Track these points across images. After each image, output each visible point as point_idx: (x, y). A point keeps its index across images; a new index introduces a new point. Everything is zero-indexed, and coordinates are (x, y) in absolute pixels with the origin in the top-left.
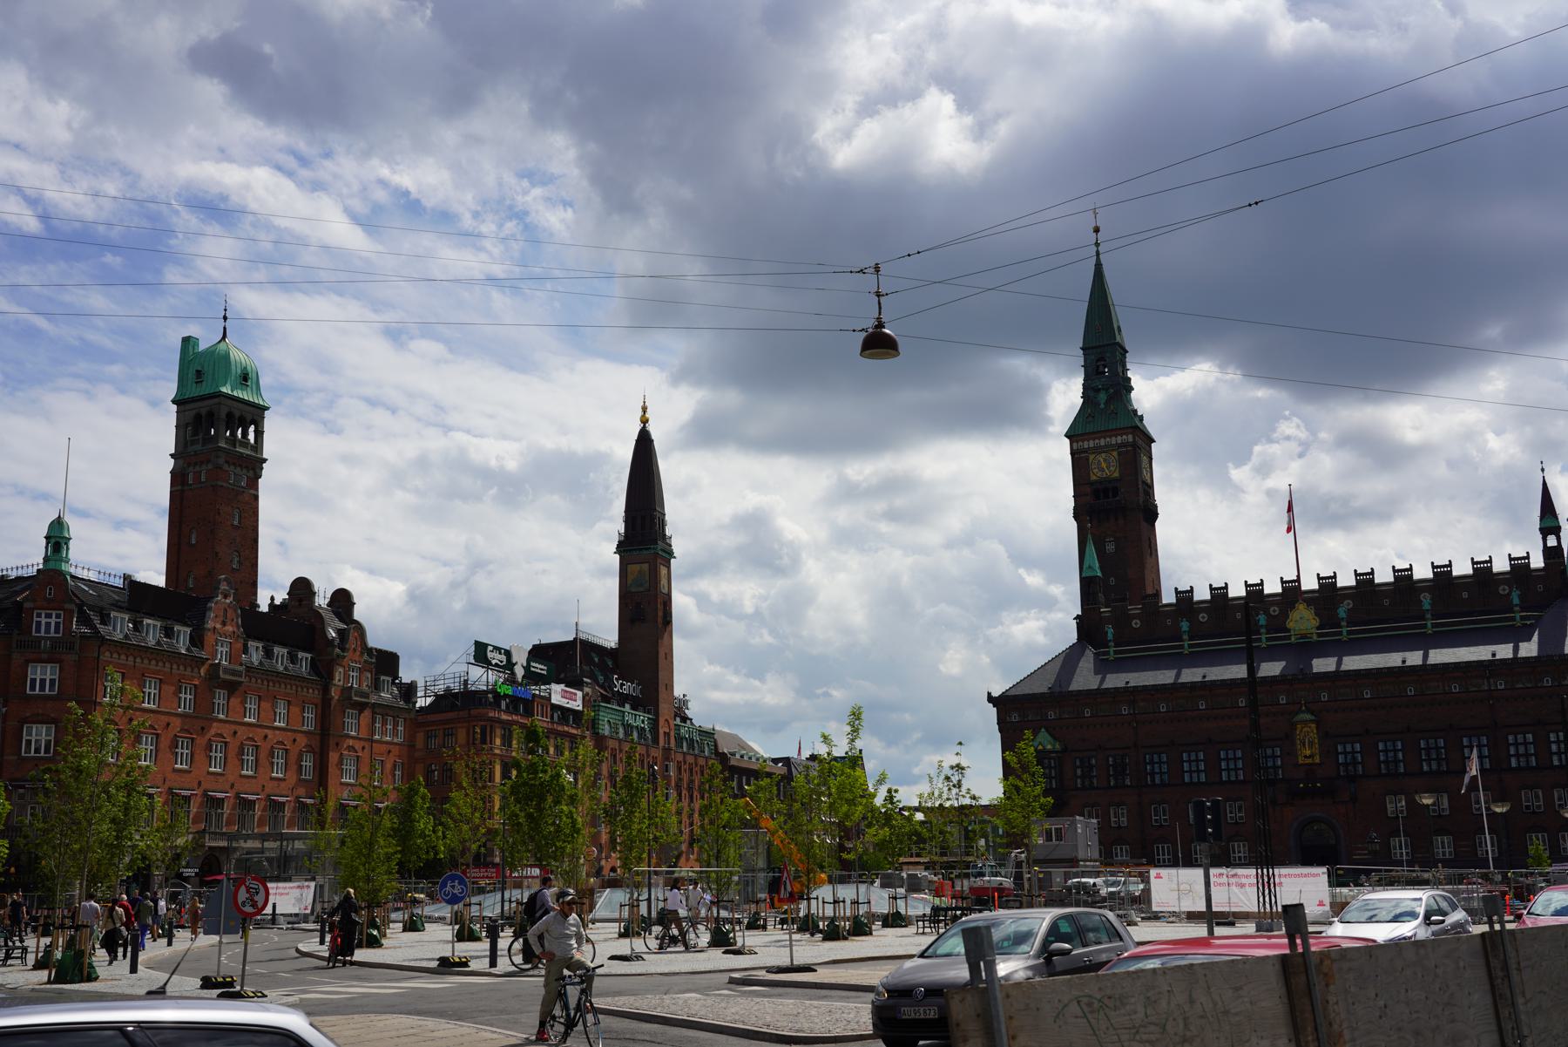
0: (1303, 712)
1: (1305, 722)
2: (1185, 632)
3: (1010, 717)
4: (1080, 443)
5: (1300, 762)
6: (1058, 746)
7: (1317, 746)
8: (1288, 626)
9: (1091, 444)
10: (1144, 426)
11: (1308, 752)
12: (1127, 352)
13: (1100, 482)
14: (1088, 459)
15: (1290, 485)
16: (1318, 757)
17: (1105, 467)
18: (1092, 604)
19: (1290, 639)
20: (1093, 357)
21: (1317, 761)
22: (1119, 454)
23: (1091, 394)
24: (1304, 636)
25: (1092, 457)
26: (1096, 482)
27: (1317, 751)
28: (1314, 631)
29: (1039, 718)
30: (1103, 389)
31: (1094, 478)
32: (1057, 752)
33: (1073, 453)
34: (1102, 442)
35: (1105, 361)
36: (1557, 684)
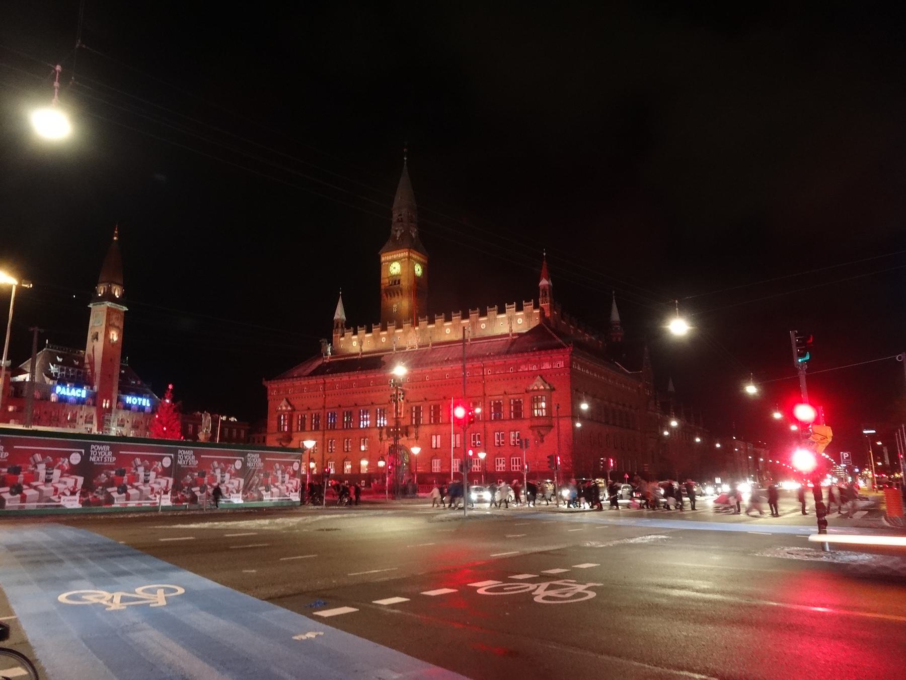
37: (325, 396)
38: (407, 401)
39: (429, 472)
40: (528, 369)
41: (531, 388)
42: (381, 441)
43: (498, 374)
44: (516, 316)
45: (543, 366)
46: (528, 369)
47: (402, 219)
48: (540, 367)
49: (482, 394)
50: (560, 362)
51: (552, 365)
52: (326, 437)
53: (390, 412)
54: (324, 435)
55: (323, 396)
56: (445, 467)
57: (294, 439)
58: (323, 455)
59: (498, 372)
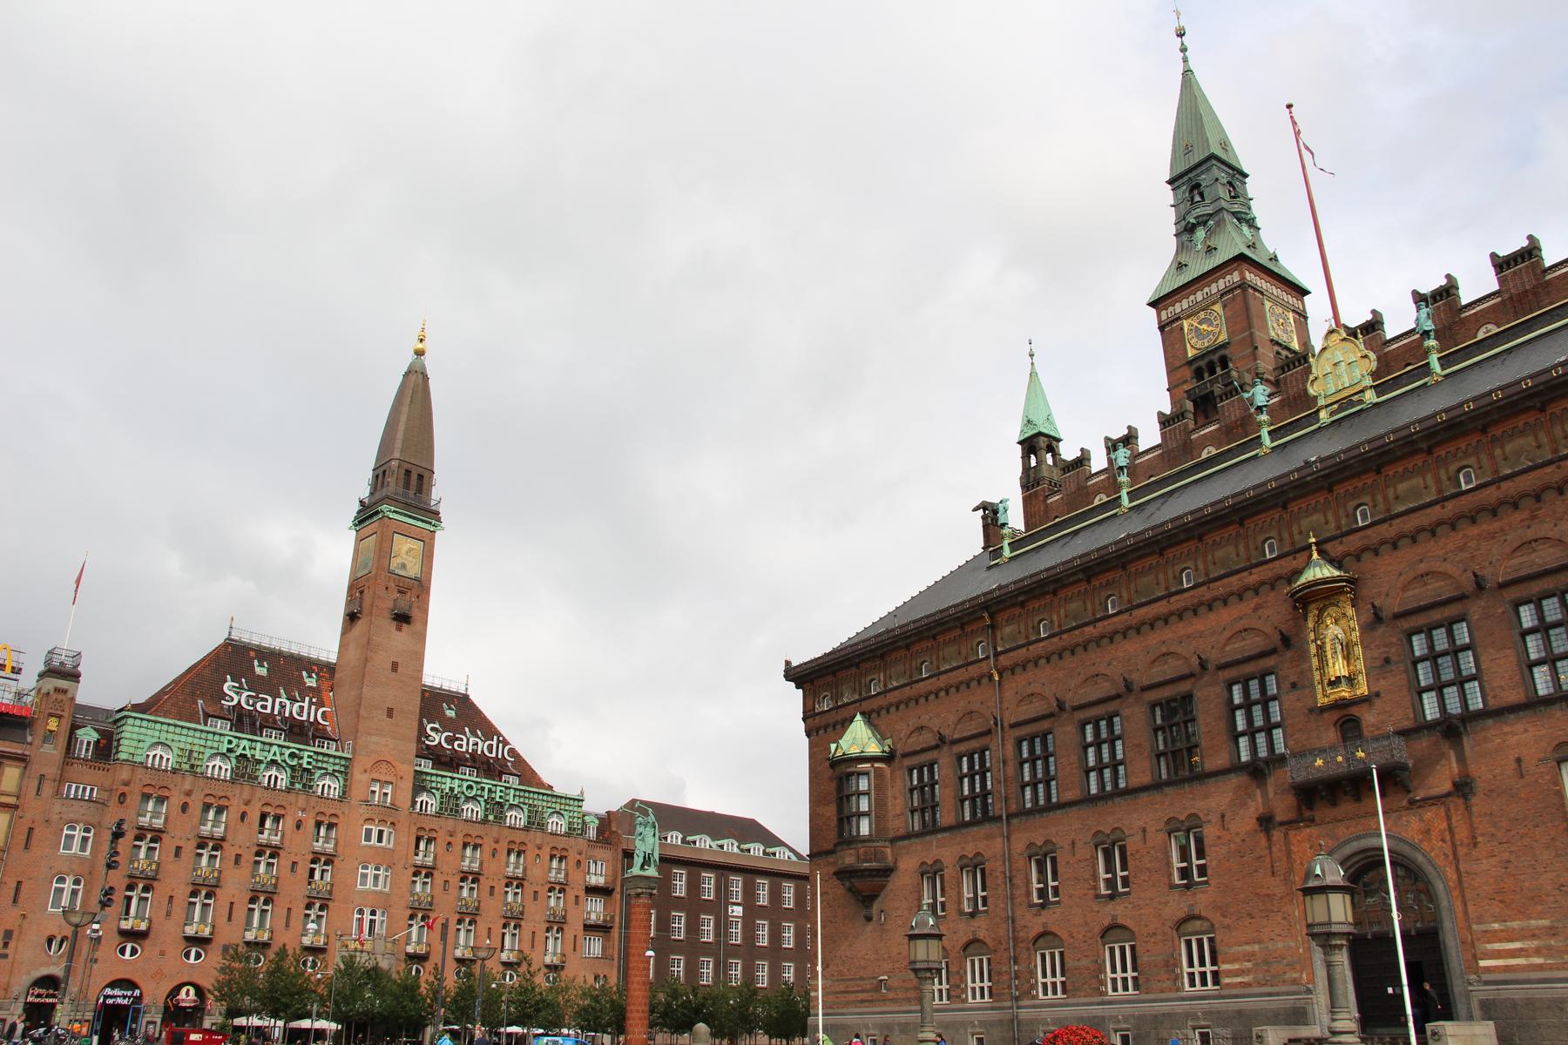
1: (1321, 595)
2: (1121, 468)
3: (819, 703)
4: (1171, 309)
5: (1322, 701)
6: (874, 748)
7: (1358, 650)
8: (1312, 391)
9: (1185, 303)
10: (1281, 267)
11: (1338, 668)
12: (1246, 176)
14: (1182, 329)
15: (1289, 106)
16: (1362, 679)
18: (1033, 486)
19: (1318, 420)
21: (1363, 690)
22: (1225, 307)
23: (1185, 237)
25: (1186, 324)
26: (1196, 359)
27: (1360, 665)
28: (1368, 382)
29: (857, 697)
30: (1199, 224)
31: (1191, 353)
32: (872, 759)
33: (1162, 328)
34: (1199, 297)
37: (1001, 676)
42: (1267, 832)
47: (1201, 195)
53: (1294, 685)
55: (991, 677)
57: (902, 865)
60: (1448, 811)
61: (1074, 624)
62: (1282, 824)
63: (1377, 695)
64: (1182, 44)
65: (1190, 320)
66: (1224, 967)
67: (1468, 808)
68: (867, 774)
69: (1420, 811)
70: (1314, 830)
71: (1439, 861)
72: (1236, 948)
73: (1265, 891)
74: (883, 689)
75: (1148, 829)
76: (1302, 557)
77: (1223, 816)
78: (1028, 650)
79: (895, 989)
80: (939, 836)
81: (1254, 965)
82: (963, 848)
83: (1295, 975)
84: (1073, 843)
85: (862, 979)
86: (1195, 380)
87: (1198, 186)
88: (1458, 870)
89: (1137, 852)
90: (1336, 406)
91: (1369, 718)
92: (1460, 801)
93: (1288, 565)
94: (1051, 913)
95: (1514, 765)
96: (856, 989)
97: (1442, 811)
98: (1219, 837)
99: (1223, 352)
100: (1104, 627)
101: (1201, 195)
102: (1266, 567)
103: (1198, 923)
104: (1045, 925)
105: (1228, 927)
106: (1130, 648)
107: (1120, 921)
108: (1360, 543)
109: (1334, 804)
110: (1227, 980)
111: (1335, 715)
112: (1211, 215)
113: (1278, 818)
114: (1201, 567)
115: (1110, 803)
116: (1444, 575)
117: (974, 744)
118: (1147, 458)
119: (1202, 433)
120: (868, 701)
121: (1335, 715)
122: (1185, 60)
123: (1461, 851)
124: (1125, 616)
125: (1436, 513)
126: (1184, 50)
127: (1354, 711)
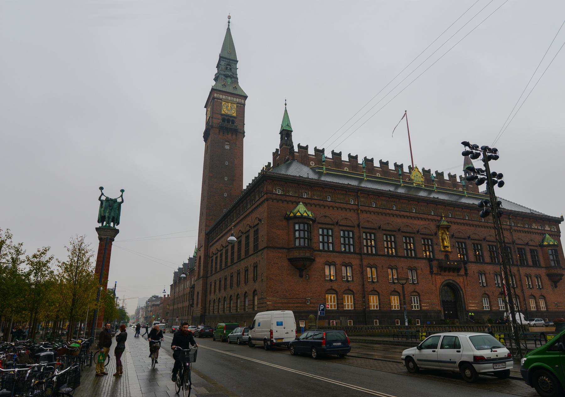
0: (444, 221)
3: (276, 190)
4: (218, 95)
5: (443, 249)
9: (224, 97)
11: (446, 244)
13: (227, 115)
14: (221, 103)
15: (406, 111)
16: (450, 247)
17: (229, 109)
20: (226, 62)
21: (450, 250)
22: (237, 107)
24: (419, 185)
25: (223, 103)
27: (449, 245)
29: (297, 195)
31: (223, 112)
34: (229, 98)
35: (231, 66)
36: (530, 227)
38: (453, 236)
39: (482, 310)
40: (538, 227)
41: (545, 243)
43: (519, 227)
44: (458, 184)
45: (545, 227)
46: (538, 227)
48: (544, 228)
49: (511, 240)
50: (554, 227)
51: (550, 227)
52: (365, 262)
53: (437, 244)
54: (361, 260)
56: (495, 305)
57: (317, 260)
58: (363, 285)
59: (519, 225)
60: (463, 278)
61: (384, 207)
62: (434, 274)
63: (452, 252)
64: (229, 21)
65: (224, 103)
66: (423, 305)
67: (467, 278)
68: (310, 225)
69: (459, 277)
70: (440, 277)
71: (462, 288)
72: (425, 300)
73: (431, 288)
74: (310, 197)
75: (404, 268)
76: (439, 218)
77: (422, 269)
78: (369, 208)
79: (314, 303)
80: (334, 254)
81: (430, 305)
82: (344, 260)
83: (438, 308)
84: (382, 266)
85: (297, 298)
86: (222, 121)
87: (230, 66)
88: (465, 290)
89: (401, 272)
90: (417, 184)
91: (451, 256)
92: (465, 277)
93: (436, 218)
94: (375, 285)
95: (473, 273)
96: (293, 302)
97: (462, 278)
98: (421, 274)
99: (234, 119)
100: (392, 212)
101: (231, 69)
102: (431, 216)
103: (415, 294)
104: (374, 288)
105: (423, 295)
106: (399, 220)
107: (396, 290)
108: (450, 220)
109: (445, 271)
110: (423, 308)
111: (444, 253)
112: (234, 77)
113: (434, 272)
114: (418, 209)
115: (393, 258)
116: (462, 233)
117: (348, 229)
118: (328, 160)
119: (345, 163)
120: (303, 199)
121: (444, 253)
122: (229, 25)
123: (466, 286)
124: (399, 212)
125: (462, 221)
126: (229, 22)
127: (448, 254)
